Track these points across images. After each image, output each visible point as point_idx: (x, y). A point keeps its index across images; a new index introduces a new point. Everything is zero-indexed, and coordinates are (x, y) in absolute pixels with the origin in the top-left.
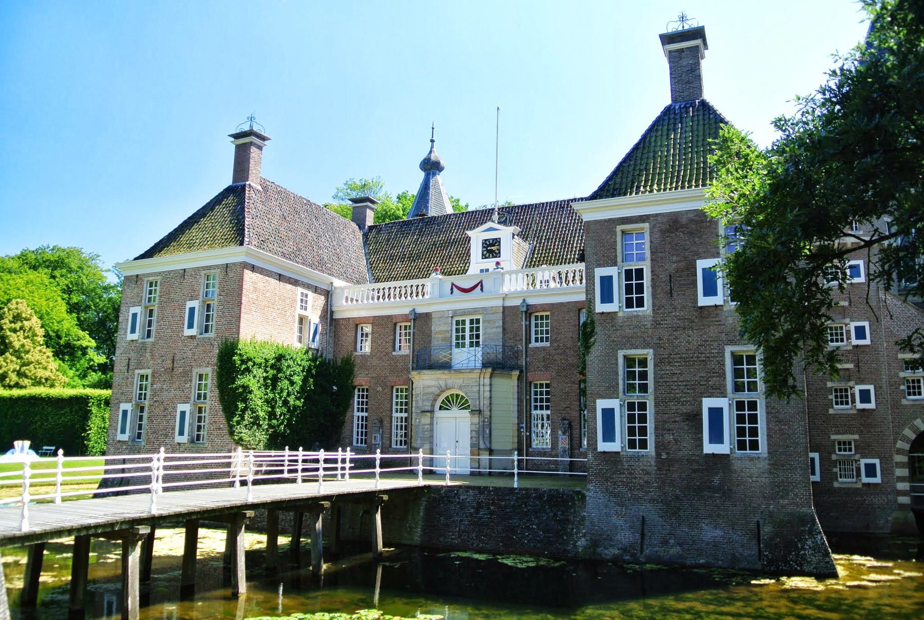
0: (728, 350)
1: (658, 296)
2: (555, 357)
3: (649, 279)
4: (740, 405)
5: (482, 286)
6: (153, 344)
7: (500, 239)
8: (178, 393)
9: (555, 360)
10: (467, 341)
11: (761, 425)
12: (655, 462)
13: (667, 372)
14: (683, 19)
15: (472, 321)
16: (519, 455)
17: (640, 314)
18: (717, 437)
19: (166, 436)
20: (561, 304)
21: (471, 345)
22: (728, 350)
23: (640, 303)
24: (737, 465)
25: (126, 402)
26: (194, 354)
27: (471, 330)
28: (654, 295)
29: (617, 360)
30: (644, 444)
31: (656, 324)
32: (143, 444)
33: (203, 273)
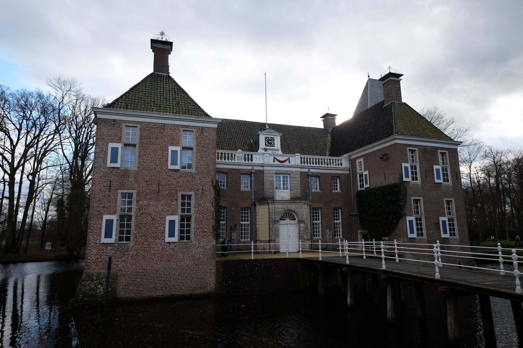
1: (422, 177)
2: (323, 197)
3: (419, 170)
5: (289, 161)
7: (274, 138)
8: (165, 207)
9: (323, 199)
10: (282, 186)
11: (456, 227)
12: (427, 241)
13: (428, 207)
14: (162, 34)
16: (254, 243)
17: (417, 183)
19: (156, 238)
21: (284, 189)
22: (445, 199)
23: (417, 180)
25: (109, 213)
28: (421, 177)
29: (411, 201)
30: (422, 235)
32: (131, 244)
33: (182, 129)
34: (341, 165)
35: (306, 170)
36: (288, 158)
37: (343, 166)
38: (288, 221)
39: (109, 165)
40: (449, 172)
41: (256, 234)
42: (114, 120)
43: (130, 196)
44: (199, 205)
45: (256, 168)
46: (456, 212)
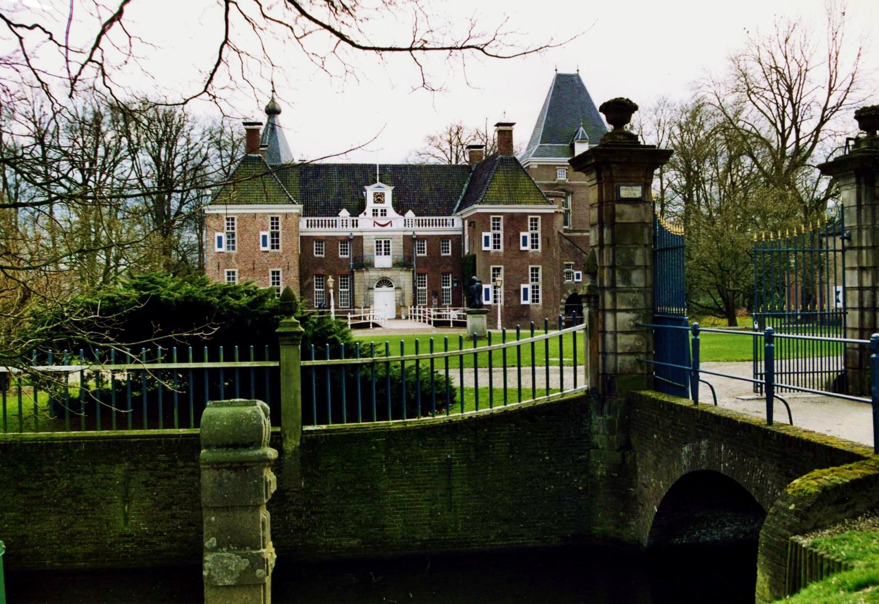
0: (530, 267)
4: (533, 287)
6: (237, 255)
10: (383, 252)
11: (540, 294)
15: (385, 242)
18: (526, 298)
20: (433, 236)
21: (385, 254)
22: (530, 267)
23: (499, 247)
24: (532, 308)
26: (268, 261)
27: (385, 246)
31: (505, 256)
34: (453, 225)
35: (411, 233)
36: (388, 221)
37: (455, 226)
38: (385, 288)
39: (218, 250)
40: (540, 239)
41: (354, 301)
42: (218, 214)
43: (234, 273)
44: (286, 279)
45: (355, 234)
46: (543, 278)
